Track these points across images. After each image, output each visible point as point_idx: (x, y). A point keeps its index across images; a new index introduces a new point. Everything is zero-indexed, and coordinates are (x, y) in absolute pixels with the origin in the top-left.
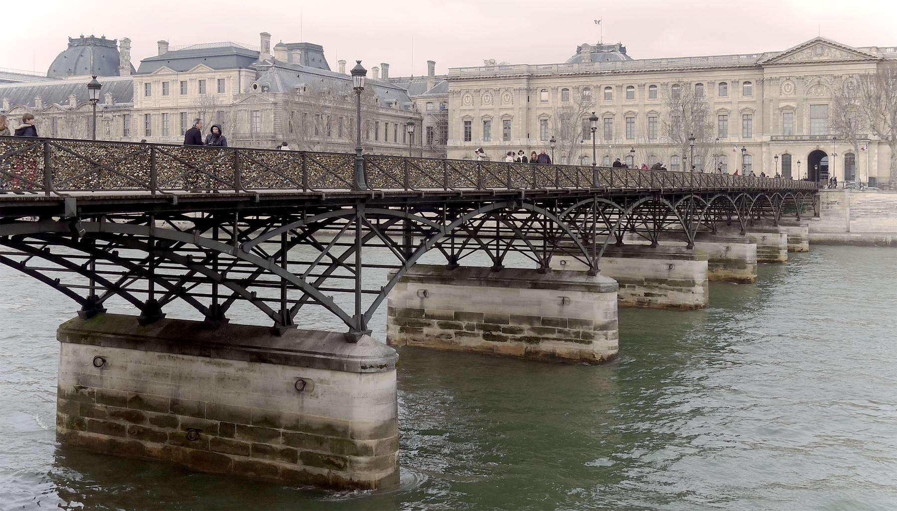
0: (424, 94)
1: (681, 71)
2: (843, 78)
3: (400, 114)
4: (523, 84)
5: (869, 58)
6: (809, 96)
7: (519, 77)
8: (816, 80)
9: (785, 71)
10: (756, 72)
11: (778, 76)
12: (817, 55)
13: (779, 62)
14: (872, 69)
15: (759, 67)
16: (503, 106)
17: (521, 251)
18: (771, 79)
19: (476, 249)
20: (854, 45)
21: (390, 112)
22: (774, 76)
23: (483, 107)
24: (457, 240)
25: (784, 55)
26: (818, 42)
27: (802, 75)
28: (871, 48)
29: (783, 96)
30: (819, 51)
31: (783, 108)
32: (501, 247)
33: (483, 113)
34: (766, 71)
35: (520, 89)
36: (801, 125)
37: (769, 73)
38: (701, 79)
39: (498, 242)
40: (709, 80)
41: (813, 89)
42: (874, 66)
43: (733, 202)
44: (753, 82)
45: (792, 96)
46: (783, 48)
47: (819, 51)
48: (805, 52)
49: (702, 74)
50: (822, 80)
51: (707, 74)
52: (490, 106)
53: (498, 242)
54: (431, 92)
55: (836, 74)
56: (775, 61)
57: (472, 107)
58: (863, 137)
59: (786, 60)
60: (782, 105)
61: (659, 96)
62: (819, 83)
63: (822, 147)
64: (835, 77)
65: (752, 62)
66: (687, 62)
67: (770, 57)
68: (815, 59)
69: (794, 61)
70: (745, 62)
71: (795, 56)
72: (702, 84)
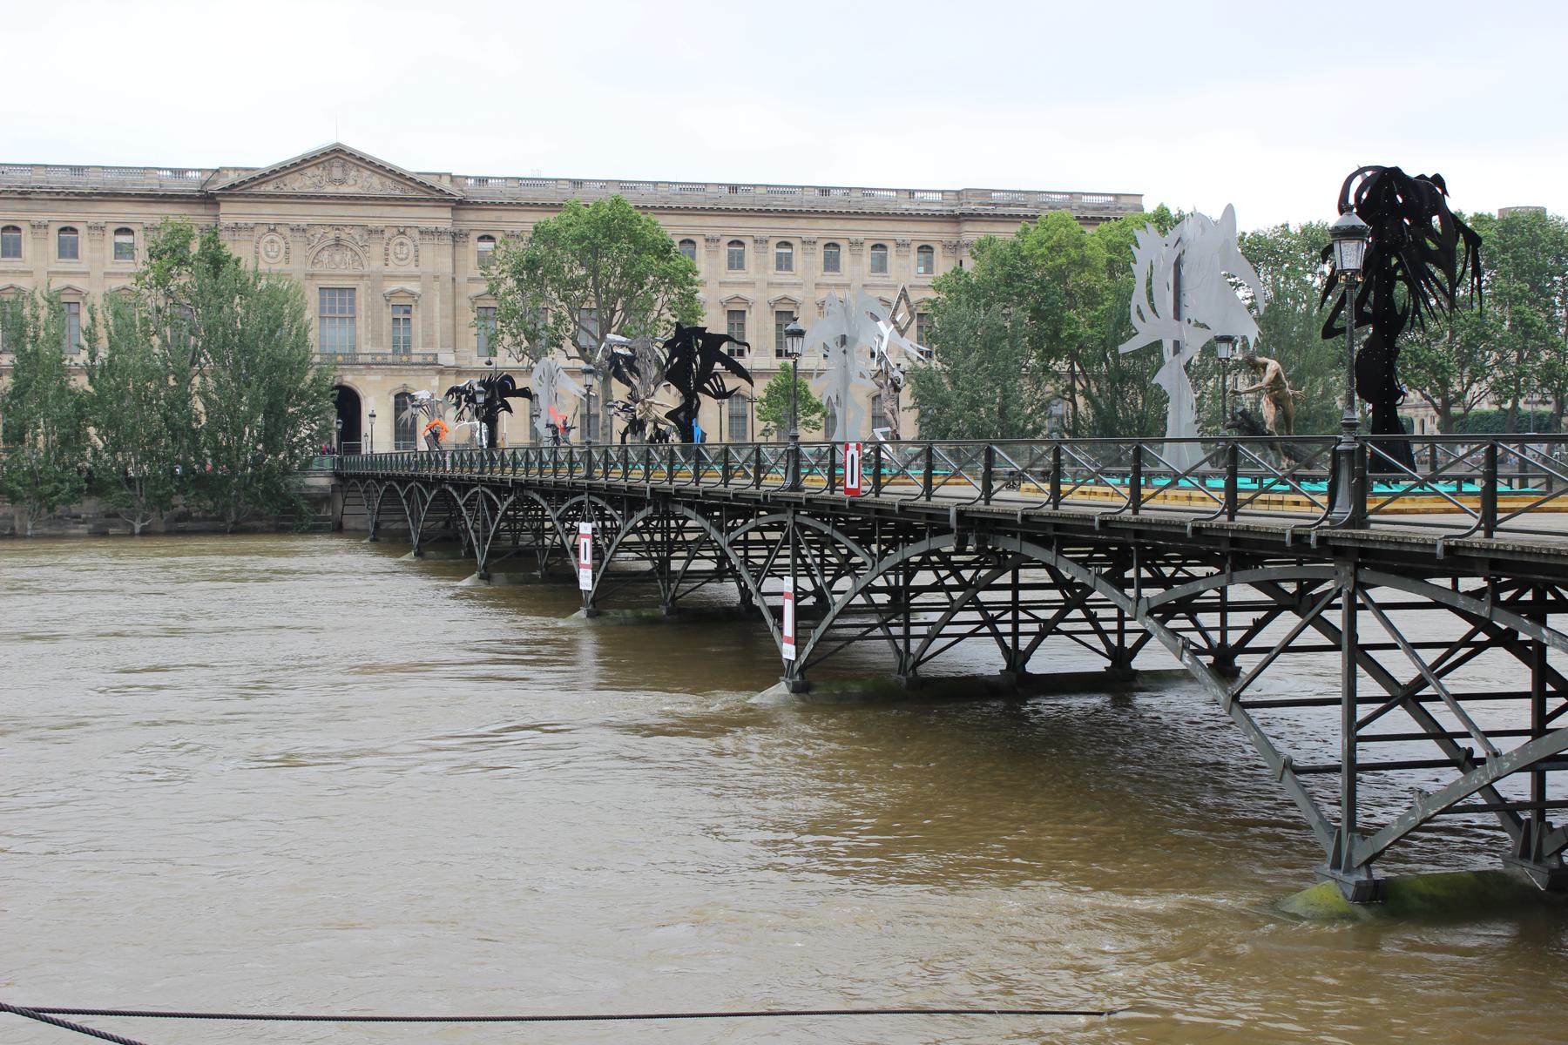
1: (24, 195)
2: (387, 235)
5: (437, 196)
6: (317, 269)
8: (332, 235)
9: (269, 213)
10: (200, 210)
11: (251, 221)
12: (333, 181)
13: (255, 190)
14: (441, 218)
15: (207, 198)
17: (1069, 634)
18: (236, 228)
19: (961, 637)
20: (410, 163)
22: (242, 221)
24: (1234, 618)
26: (337, 155)
27: (303, 223)
28: (440, 175)
30: (337, 173)
32: (1022, 628)
34: (224, 208)
37: (230, 213)
38: (71, 217)
39: (1015, 616)
40: (92, 220)
41: (326, 253)
42: (446, 213)
43: (461, 502)
46: (265, 160)
47: (337, 173)
48: (309, 172)
49: (74, 206)
50: (343, 236)
51: (86, 207)
53: (1015, 616)
55: (373, 224)
56: (247, 187)
58: (430, 359)
59: (269, 188)
62: (338, 243)
64: (370, 232)
65: (192, 183)
66: (41, 175)
67: (233, 178)
68: (330, 189)
69: (287, 190)
70: (176, 186)
71: (287, 179)
72: (74, 230)
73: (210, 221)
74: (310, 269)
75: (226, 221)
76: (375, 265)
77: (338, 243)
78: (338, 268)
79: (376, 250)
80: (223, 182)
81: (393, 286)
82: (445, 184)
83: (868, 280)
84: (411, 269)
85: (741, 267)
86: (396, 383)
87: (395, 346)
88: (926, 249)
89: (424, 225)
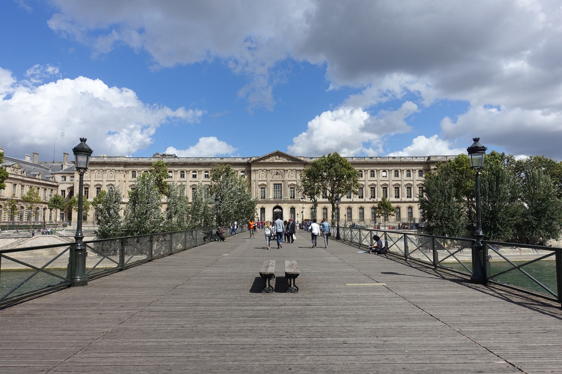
0: (60, 172)
3: (42, 182)
4: (121, 168)
6: (273, 179)
7: (118, 164)
12: (276, 159)
15: (248, 165)
16: (109, 179)
18: (255, 171)
21: (34, 180)
22: (256, 168)
23: (97, 179)
25: (261, 159)
29: (261, 179)
31: (261, 185)
33: (97, 183)
35: (119, 171)
36: (269, 193)
44: (246, 172)
45: (265, 179)
46: (261, 156)
47: (278, 157)
52: (101, 179)
54: (65, 170)
55: (286, 168)
57: (89, 179)
60: (260, 183)
61: (197, 176)
63: (279, 204)
64: (285, 171)
65: (245, 161)
68: (276, 161)
73: (248, 169)
74: (271, 179)
75: (252, 169)
76: (286, 178)
77: (277, 174)
78: (278, 178)
79: (287, 175)
80: (252, 160)
81: (290, 183)
82: (302, 159)
83: (405, 179)
84: (294, 179)
85: (374, 176)
86: (291, 205)
87: (291, 197)
88: (420, 171)
89: (297, 168)
